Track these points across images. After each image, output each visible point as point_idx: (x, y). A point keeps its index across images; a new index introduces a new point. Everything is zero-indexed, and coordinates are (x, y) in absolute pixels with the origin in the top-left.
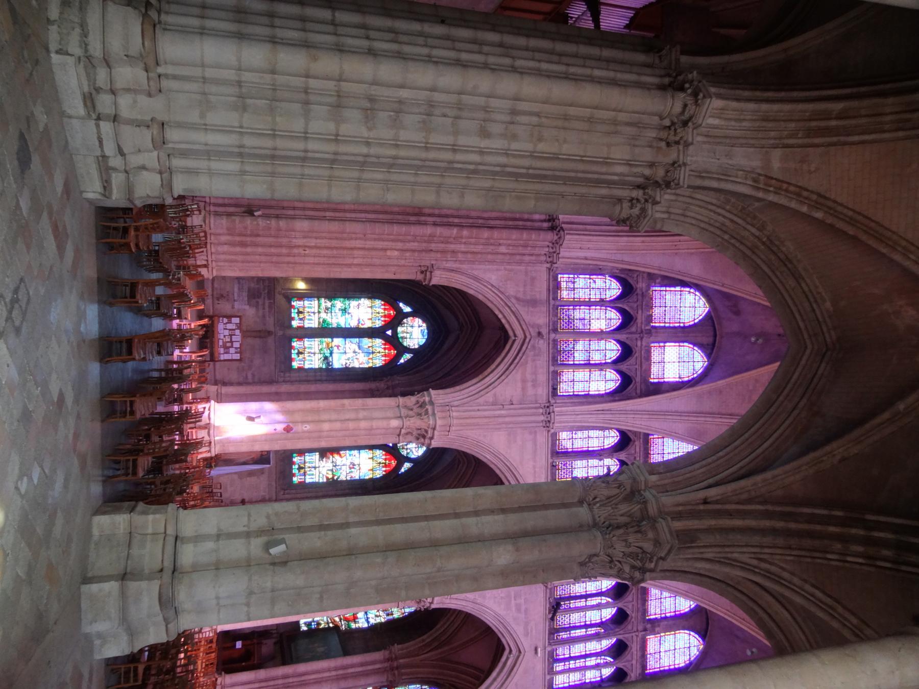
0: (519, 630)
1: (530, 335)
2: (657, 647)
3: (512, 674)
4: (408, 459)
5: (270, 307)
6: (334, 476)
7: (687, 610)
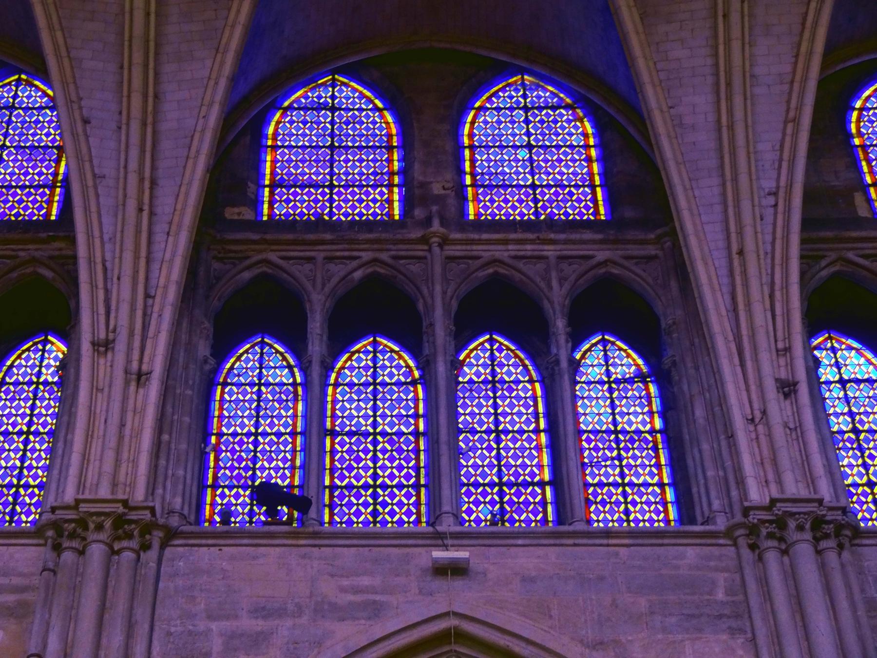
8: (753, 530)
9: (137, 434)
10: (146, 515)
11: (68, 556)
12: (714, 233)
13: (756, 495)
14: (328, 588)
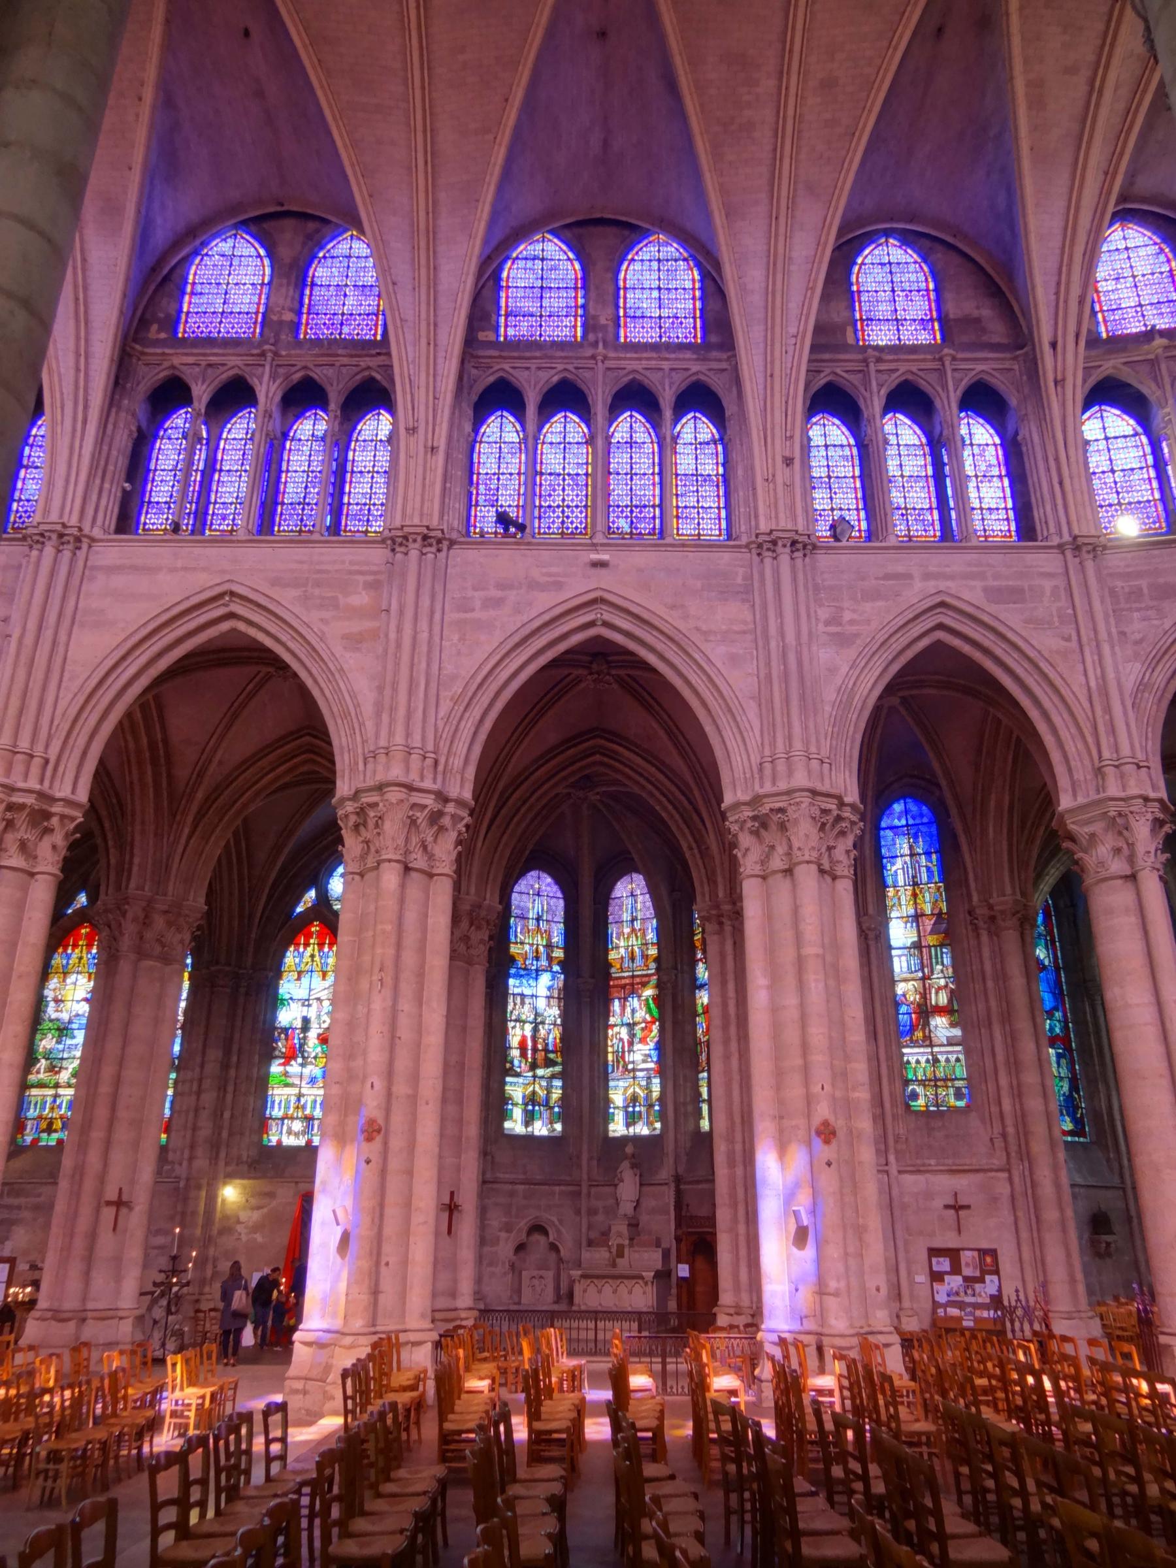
0: (545, 603)
2: (647, 323)
3: (646, 615)
5: (18, 1194)
7: (577, 266)
8: (760, 546)
9: (433, 484)
10: (439, 534)
11: (399, 556)
12: (758, 360)
13: (764, 527)
14: (536, 573)
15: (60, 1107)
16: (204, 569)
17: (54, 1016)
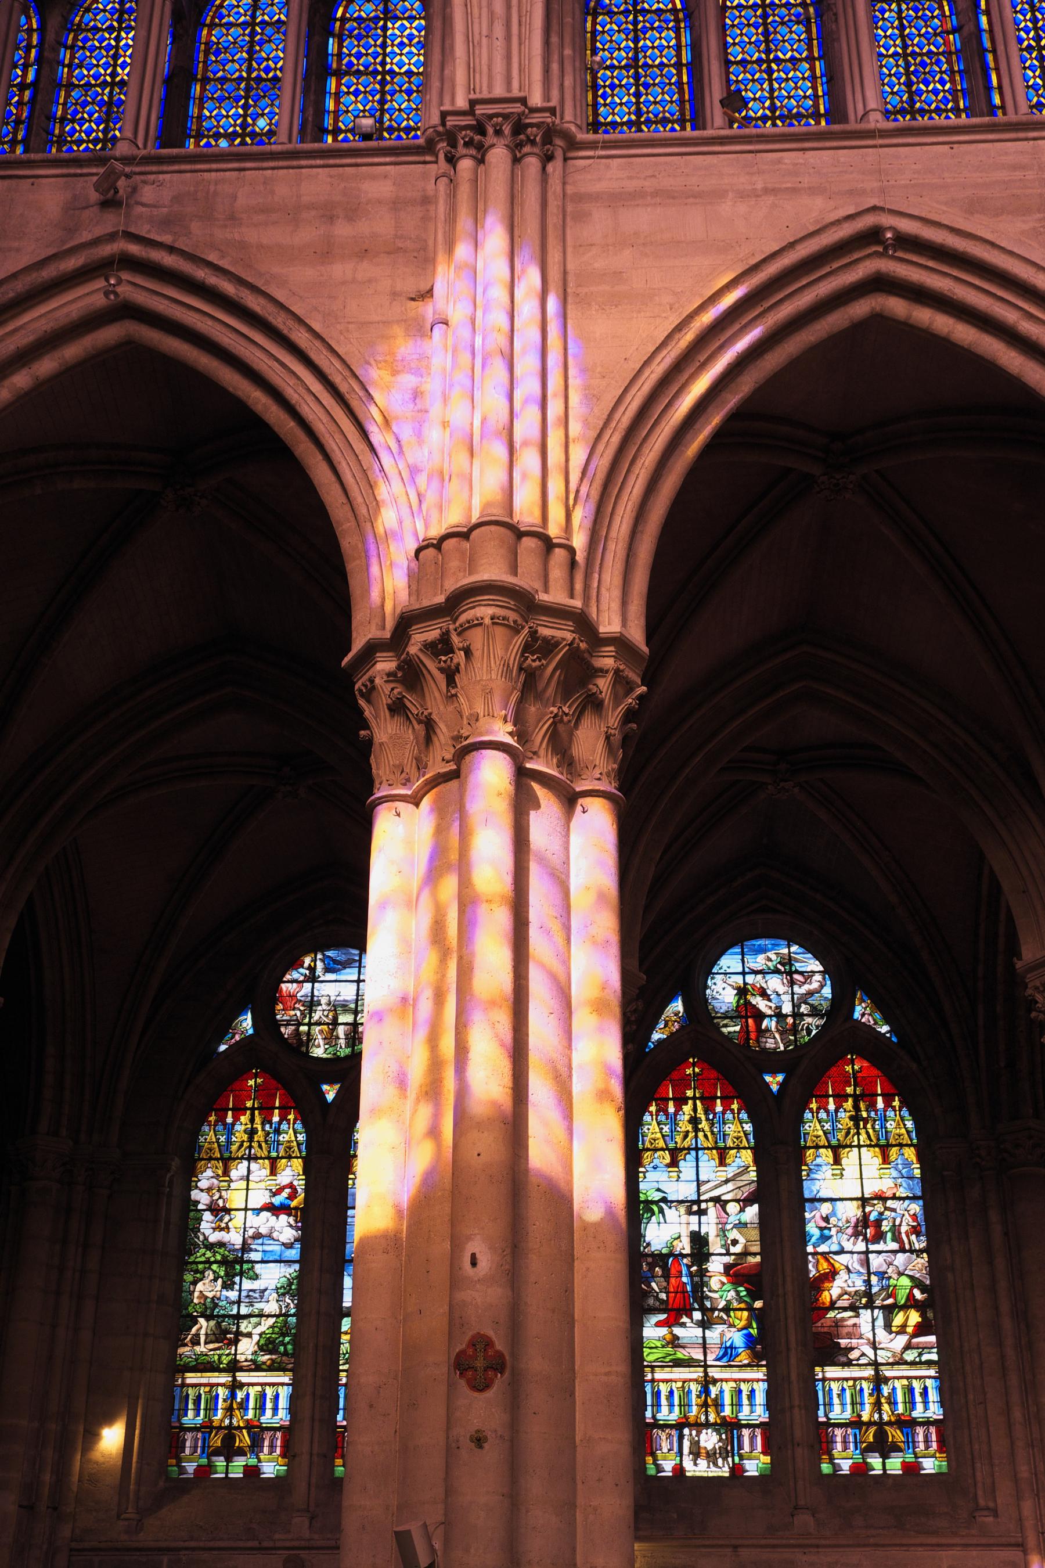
1: (112, 237)
4: (841, 1004)
6: (911, 1303)
15: (244, 1406)
16: (813, 191)
17: (214, 1237)
